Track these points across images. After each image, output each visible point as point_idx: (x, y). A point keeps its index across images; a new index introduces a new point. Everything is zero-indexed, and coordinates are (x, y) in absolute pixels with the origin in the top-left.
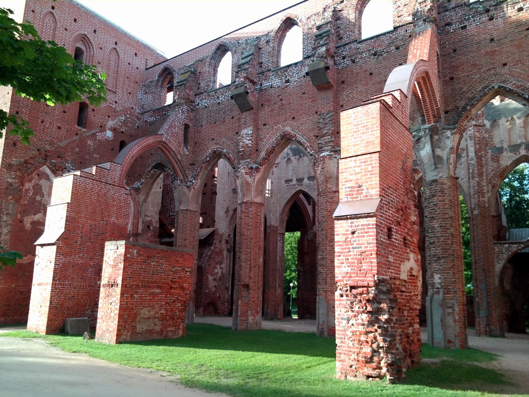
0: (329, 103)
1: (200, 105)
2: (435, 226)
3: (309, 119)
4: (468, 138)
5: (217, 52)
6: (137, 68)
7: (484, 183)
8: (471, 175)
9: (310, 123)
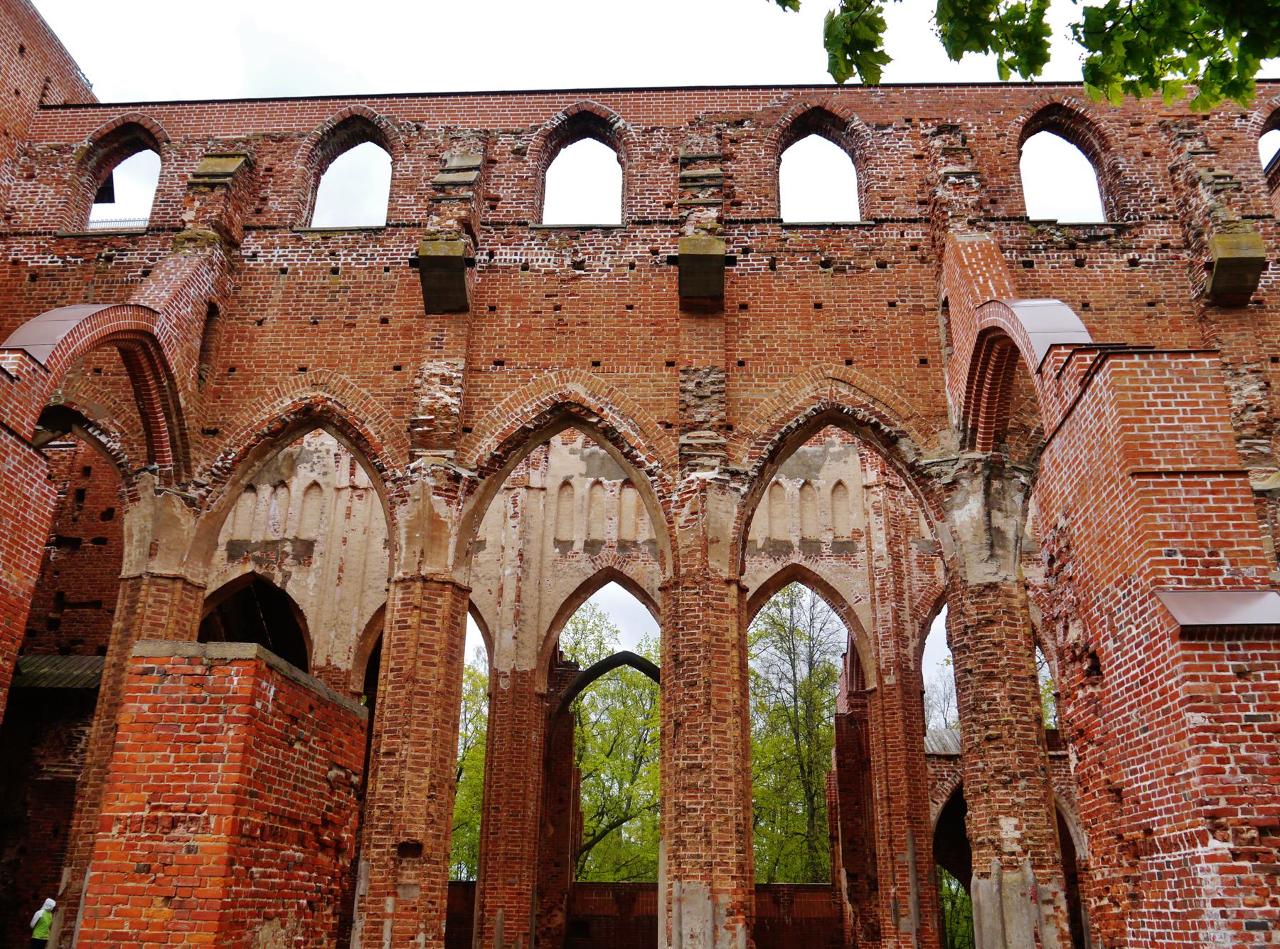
1: (260, 260)
2: (997, 695)
4: (872, 511)
5: (338, 132)
6: (17, 93)
7: (906, 615)
8: (877, 593)
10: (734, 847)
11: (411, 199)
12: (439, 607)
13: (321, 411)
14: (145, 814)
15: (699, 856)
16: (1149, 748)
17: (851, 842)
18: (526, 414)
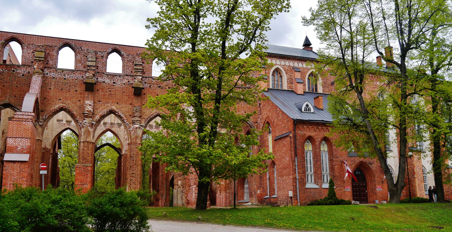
1: (49, 75)
11: (80, 65)
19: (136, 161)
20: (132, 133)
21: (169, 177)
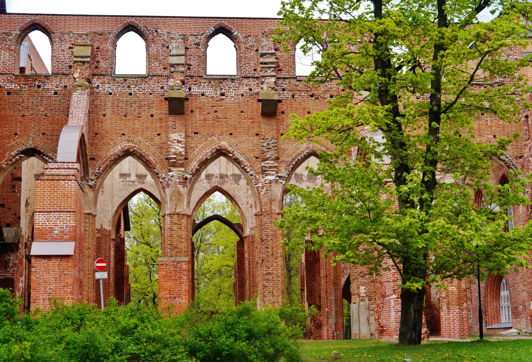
0: (272, 130)
1: (101, 89)
3: (249, 139)
9: (250, 143)
10: (281, 297)
11: (157, 64)
12: (183, 223)
13: (132, 151)
14: (168, 296)
15: (270, 300)
16: (386, 275)
17: (310, 292)
18: (207, 153)
19: (272, 248)
20: (262, 193)
21: (341, 279)
